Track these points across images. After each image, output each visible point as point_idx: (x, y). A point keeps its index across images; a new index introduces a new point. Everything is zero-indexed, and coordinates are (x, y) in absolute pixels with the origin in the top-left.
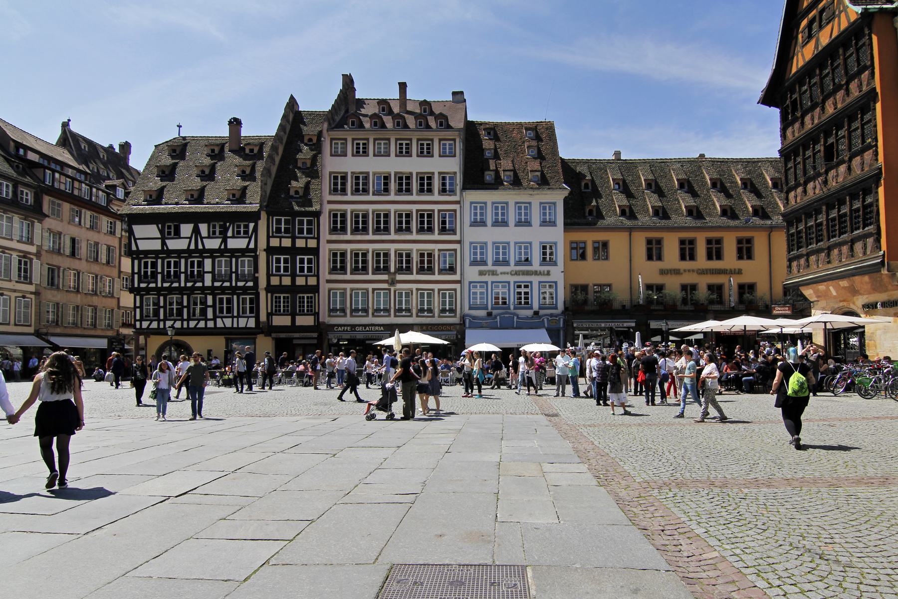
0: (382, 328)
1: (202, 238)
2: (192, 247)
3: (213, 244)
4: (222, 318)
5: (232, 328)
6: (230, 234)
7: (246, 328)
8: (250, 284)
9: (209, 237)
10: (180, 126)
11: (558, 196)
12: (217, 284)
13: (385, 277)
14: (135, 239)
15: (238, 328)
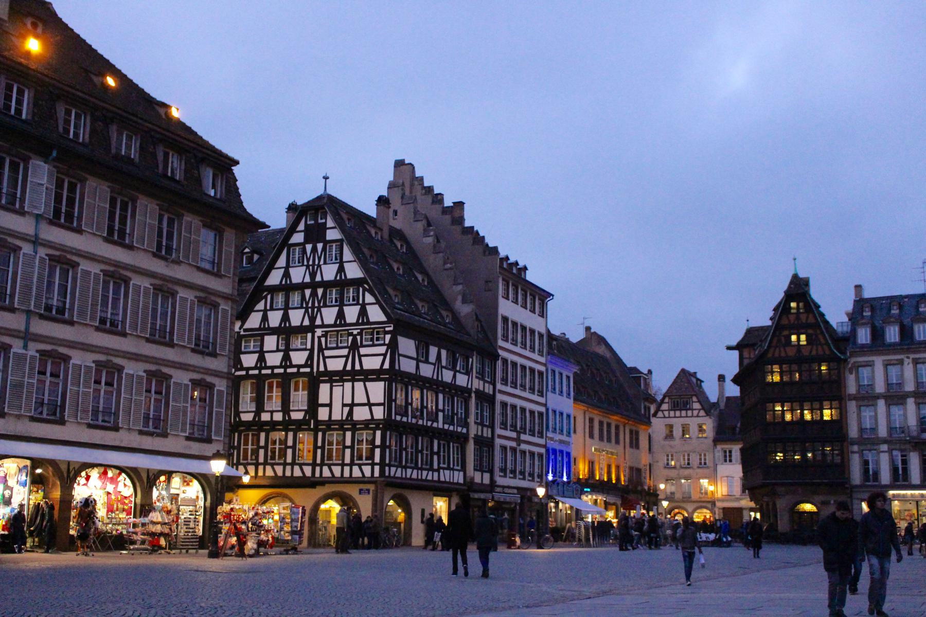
0: (515, 491)
1: (442, 367)
2: (435, 377)
3: (447, 376)
4: (444, 469)
5: (449, 483)
6: (458, 368)
7: (458, 484)
8: (464, 431)
9: (446, 368)
10: (326, 178)
11: (569, 371)
12: (446, 427)
13: (514, 435)
14: (400, 355)
15: (453, 483)
